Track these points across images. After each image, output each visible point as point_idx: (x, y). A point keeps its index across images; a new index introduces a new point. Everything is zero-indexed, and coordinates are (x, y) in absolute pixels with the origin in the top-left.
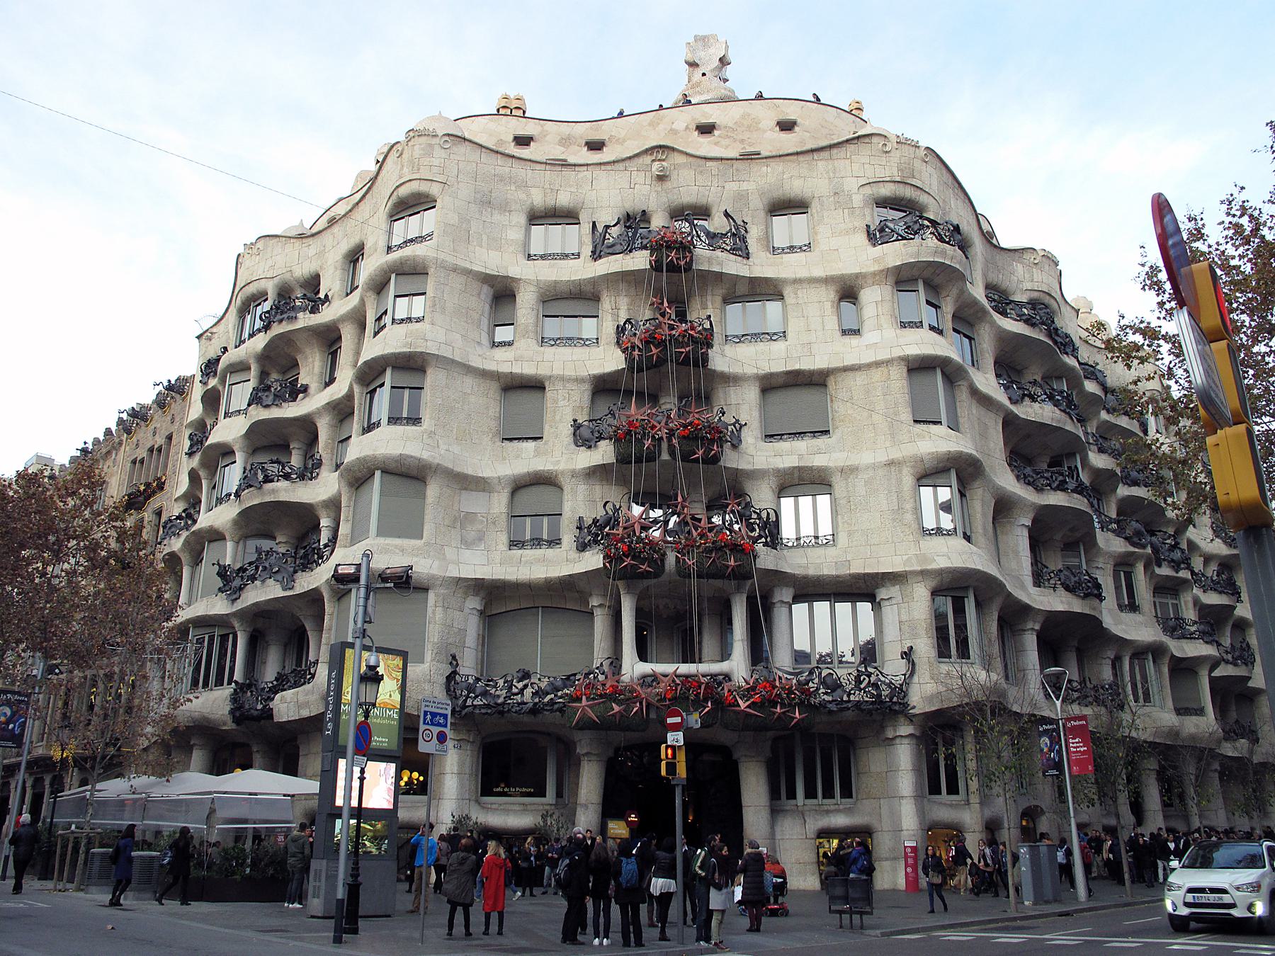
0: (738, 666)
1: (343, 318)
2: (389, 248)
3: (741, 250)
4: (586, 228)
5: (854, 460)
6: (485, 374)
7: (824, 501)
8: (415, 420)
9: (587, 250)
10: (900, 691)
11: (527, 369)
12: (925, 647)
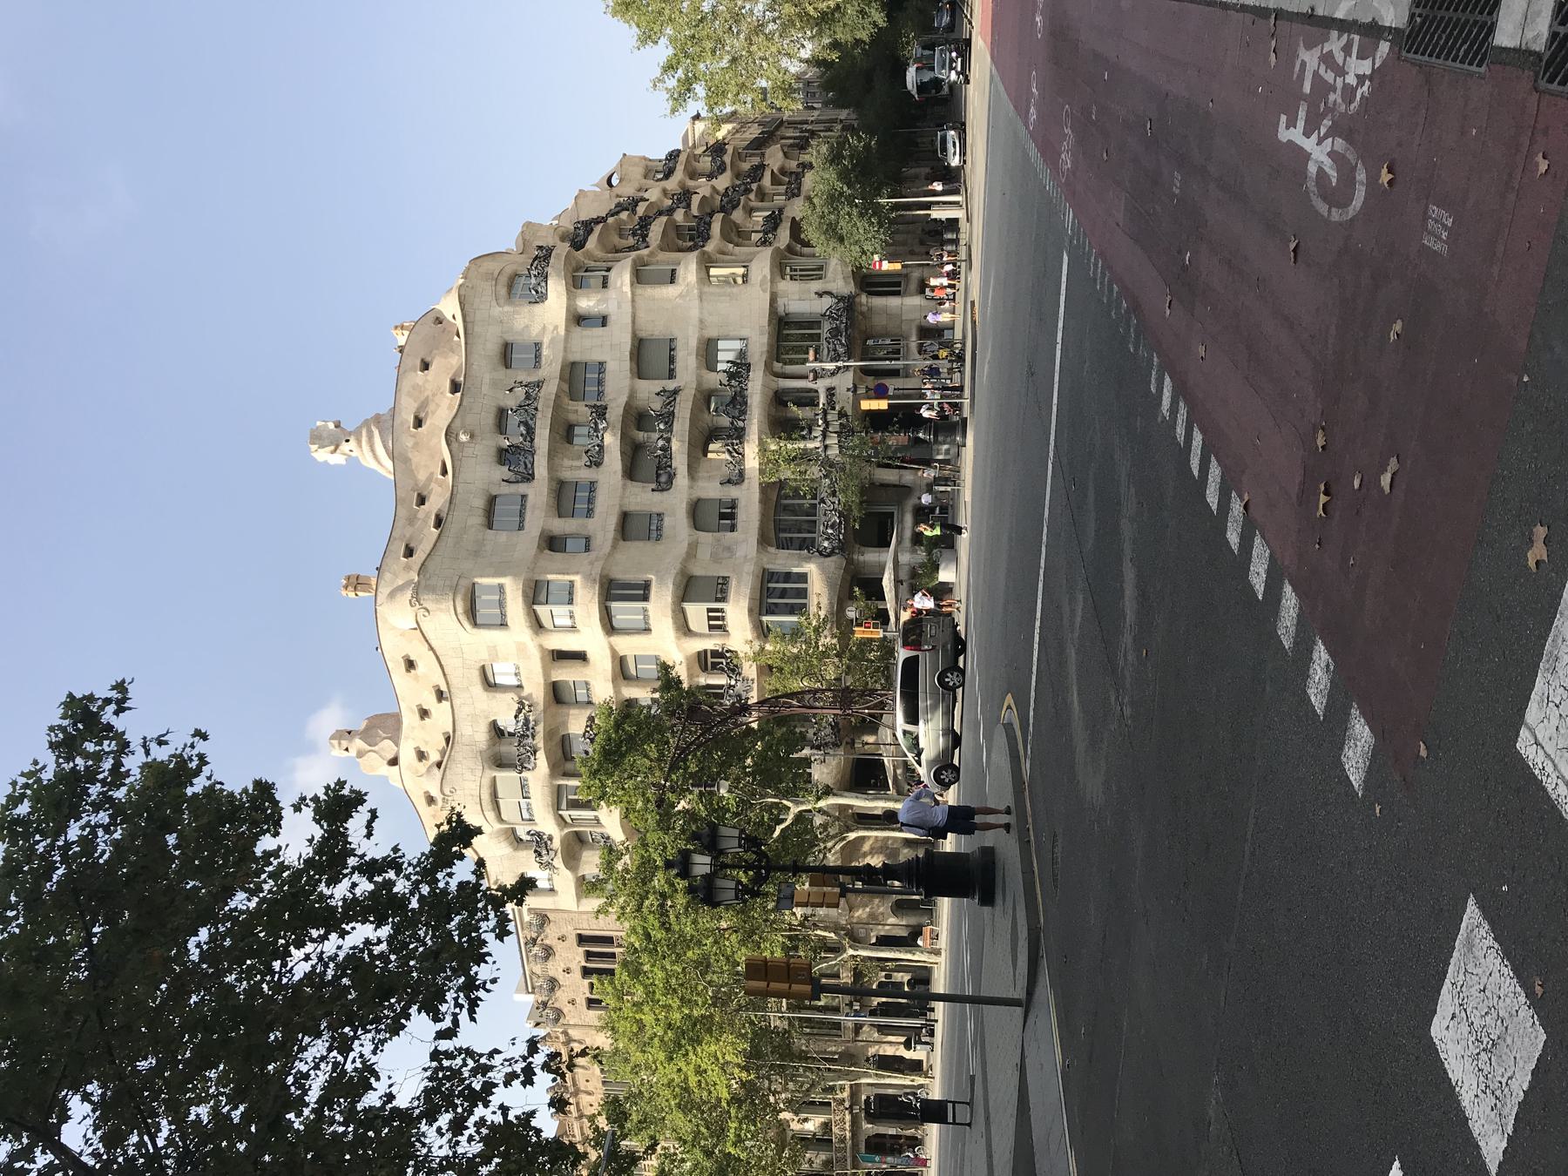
0: (821, 386)
1: (546, 674)
2: (504, 625)
3: (539, 385)
4: (507, 489)
5: (695, 321)
6: (614, 547)
7: (721, 345)
8: (646, 586)
9: (522, 488)
10: (841, 299)
11: (613, 522)
12: (816, 286)
